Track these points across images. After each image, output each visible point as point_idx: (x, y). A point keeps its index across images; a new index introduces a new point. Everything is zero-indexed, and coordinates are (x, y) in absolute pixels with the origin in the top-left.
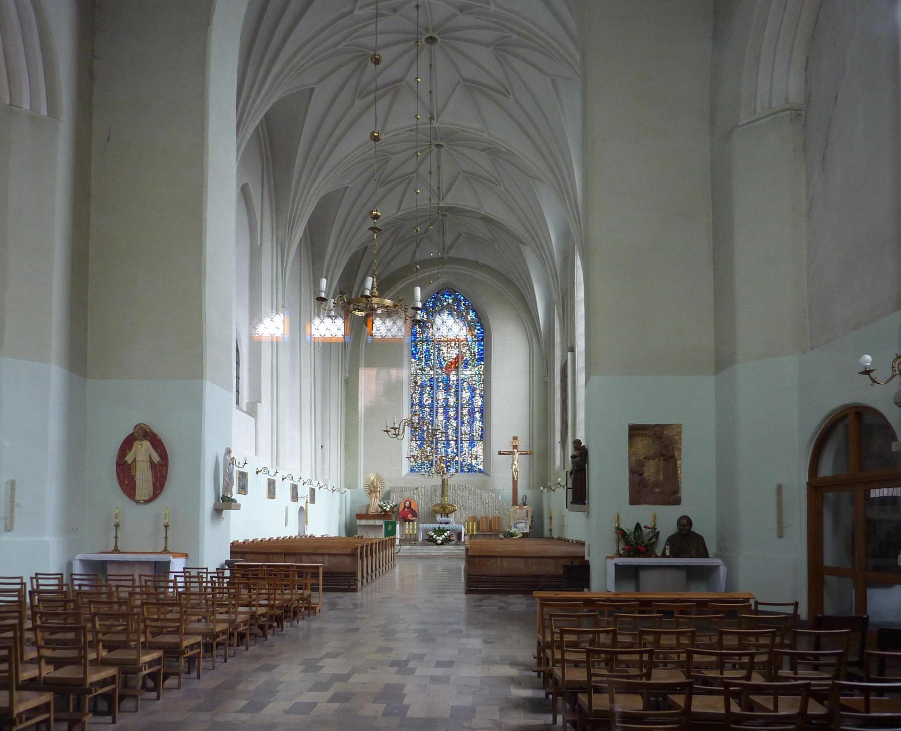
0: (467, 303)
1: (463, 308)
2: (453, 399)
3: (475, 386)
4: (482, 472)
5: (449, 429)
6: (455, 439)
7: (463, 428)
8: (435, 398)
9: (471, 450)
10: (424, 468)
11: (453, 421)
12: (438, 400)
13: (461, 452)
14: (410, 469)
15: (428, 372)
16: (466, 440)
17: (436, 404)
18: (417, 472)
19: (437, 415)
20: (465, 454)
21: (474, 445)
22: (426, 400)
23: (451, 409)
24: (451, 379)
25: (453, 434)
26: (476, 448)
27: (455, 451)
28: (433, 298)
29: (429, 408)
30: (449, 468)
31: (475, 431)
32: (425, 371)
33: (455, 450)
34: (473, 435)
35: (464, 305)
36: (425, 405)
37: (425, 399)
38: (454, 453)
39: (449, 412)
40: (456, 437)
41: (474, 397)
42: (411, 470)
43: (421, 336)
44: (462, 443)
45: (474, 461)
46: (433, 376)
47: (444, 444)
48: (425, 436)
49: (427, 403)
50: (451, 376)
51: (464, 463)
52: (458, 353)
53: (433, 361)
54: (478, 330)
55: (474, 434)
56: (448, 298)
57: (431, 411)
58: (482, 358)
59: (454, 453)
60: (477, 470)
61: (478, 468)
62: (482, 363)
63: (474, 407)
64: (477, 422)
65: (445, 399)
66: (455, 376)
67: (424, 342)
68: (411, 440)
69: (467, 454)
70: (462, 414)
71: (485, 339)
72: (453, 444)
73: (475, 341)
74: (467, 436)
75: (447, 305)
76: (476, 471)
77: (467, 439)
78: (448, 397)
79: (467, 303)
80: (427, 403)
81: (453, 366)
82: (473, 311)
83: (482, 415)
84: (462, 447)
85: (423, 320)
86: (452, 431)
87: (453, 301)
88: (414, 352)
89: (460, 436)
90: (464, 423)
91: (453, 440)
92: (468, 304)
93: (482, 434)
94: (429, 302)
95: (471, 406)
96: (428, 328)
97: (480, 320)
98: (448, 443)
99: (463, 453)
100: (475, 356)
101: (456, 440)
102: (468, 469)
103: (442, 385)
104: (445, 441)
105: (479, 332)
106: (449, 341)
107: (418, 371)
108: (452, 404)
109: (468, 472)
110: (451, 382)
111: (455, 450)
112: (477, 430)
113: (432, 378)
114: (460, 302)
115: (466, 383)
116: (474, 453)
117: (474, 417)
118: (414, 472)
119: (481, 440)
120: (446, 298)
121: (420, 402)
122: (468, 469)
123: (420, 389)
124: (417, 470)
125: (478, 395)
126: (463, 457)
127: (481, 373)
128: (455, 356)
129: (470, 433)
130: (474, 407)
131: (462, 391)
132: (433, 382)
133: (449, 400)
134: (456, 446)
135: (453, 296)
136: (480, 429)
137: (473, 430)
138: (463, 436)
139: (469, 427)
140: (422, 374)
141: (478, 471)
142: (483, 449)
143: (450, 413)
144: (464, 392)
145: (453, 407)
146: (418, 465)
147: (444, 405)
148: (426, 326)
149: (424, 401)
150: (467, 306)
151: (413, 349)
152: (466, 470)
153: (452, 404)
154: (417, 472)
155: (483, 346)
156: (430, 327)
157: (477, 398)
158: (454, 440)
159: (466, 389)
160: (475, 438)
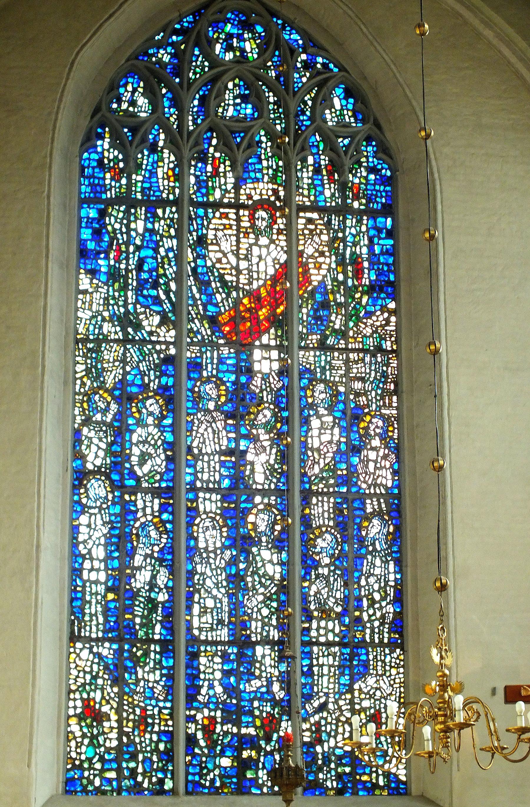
0: (320, 60)
1: (304, 80)
2: (263, 458)
3: (363, 400)
4: (406, 793)
5: (246, 589)
6: (275, 634)
7: (314, 588)
8: (184, 450)
9: (351, 690)
10: (133, 773)
11: (266, 554)
12: (196, 458)
13: (308, 698)
14: (61, 779)
15: (151, 333)
16: (329, 644)
17: (188, 478)
18: (98, 791)
19: (190, 524)
20: (323, 707)
21: (366, 665)
22: (141, 464)
23: (258, 499)
24: (256, 367)
25: (265, 612)
26: (371, 681)
27: (280, 695)
28: (176, 32)
29: (156, 493)
30: (249, 775)
31: (365, 603)
32: (138, 327)
33: (276, 687)
34: (358, 620)
35: (307, 66)
36: (138, 479)
37: (136, 451)
38: (275, 703)
39: (246, 512)
40: (280, 627)
41: (356, 450)
42: (69, 781)
43: (124, 181)
44: (309, 655)
45: (365, 739)
46: (172, 351)
47: (225, 657)
48: (138, 620)
49: (146, 468)
50: (257, 354)
51: (319, 749)
52: (283, 257)
53: (173, 286)
54: (372, 170)
55: (365, 617)
56: (240, 38)
57: (163, 508)
58: (391, 284)
59: (275, 703)
60: (381, 783)
61: (387, 775)
62: (392, 305)
63: (362, 497)
64: (378, 562)
65: (230, 452)
66: (274, 354)
67: (133, 204)
68: (73, 638)
69: (331, 706)
70: (306, 521)
71: (401, 209)
72: (268, 661)
73: (359, 214)
74: (330, 625)
75: (236, 61)
76: (376, 786)
77: (331, 637)
78: (243, 444)
79: (320, 60)
80: (146, 468)
81: (263, 313)
82: (348, 94)
83: (398, 528)
84: (309, 673)
85: (134, 115)
86: (261, 598)
87: (262, 50)
88: (91, 245)
89: (299, 625)
90: (317, 565)
91: (266, 641)
92: (324, 65)
93: (399, 618)
94: (160, 45)
95: (344, 489)
96: (153, 149)
97: (377, 125)
98: (240, 655)
99: (316, 704)
100: (358, 273)
101: (280, 642)
102: (339, 777)
103: (214, 393)
104: (230, 643)
105: (372, 177)
106: (244, 207)
107: (107, 327)
108: (259, 478)
109: (340, 792)
110: (257, 381)
111: (276, 687)
112: (377, 596)
113: (169, 360)
114: (293, 53)
115: (321, 387)
116: (366, 704)
117: (361, 540)
118: (85, 791)
119: (393, 645)
120: (230, 36)
121: (115, 464)
122: (339, 777)
123: (114, 407)
124: (97, 782)
125: (376, 442)
126: (312, 720)
127: (388, 345)
128: (271, 271)
129: (345, 612)
130: (362, 497)
131: (306, 421)
132: (176, 376)
133: (250, 457)
134: (283, 667)
135: (259, 29)
136: (391, 592)
137: (359, 599)
138: (314, 625)
139: (339, 583)
140: (125, 341)
141: (387, 786)
142: (405, 684)
143: (251, 518)
144: (315, 423)
145: (264, 493)
146: (102, 759)
147: (226, 483)
148: (144, 140)
149: (134, 459)
150: (319, 73)
151: (86, 234)
152: (329, 784)
153: (259, 478)
154: (98, 791)
155: (390, 234)
156: (161, 143)
157: (372, 455)
158: (272, 643)
159: (322, 411)
160: (368, 631)
